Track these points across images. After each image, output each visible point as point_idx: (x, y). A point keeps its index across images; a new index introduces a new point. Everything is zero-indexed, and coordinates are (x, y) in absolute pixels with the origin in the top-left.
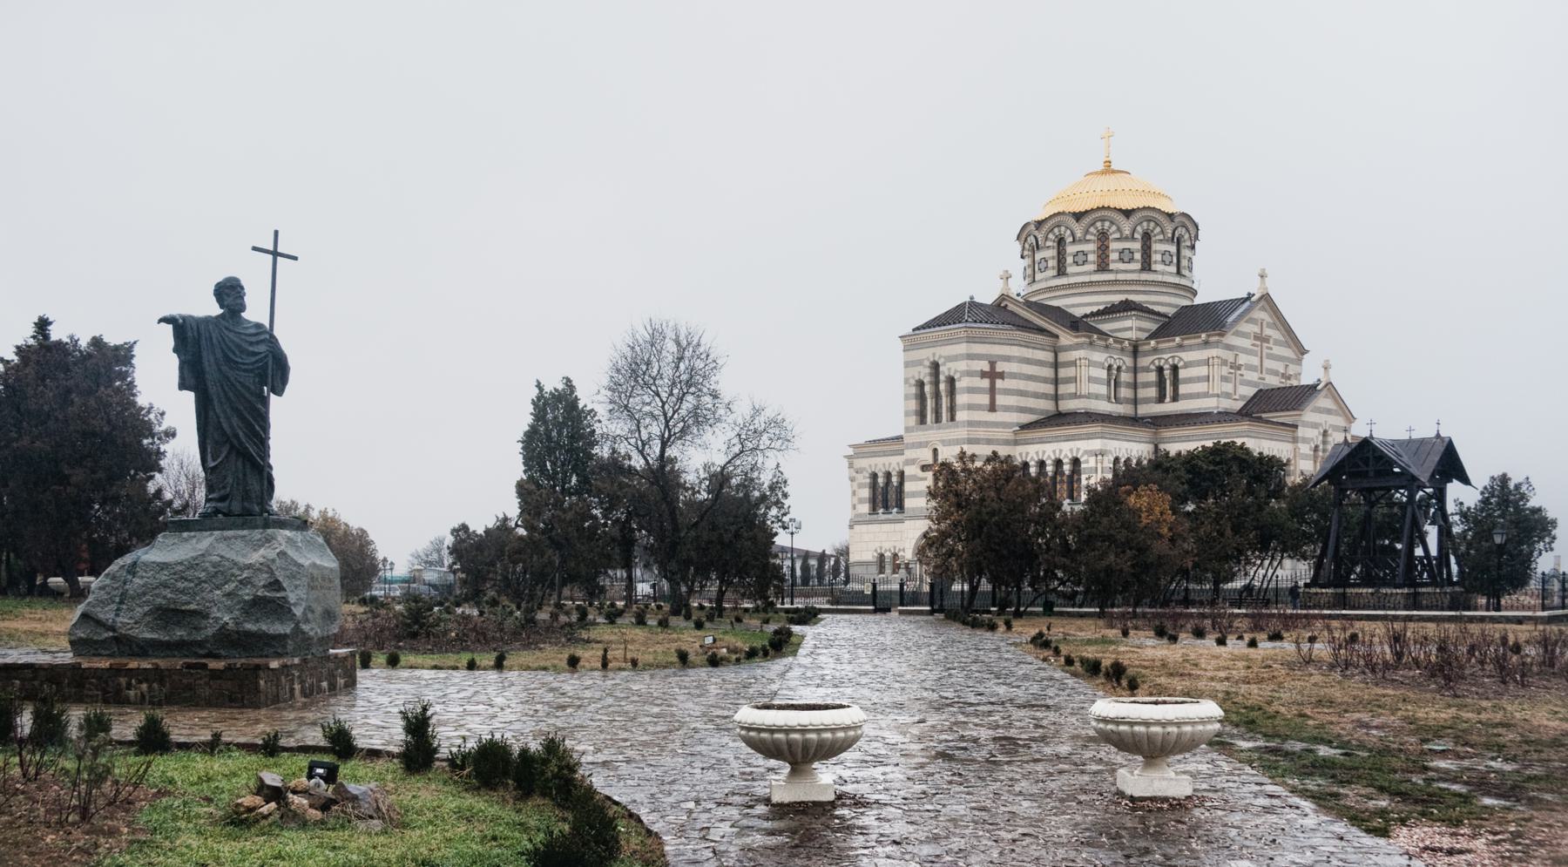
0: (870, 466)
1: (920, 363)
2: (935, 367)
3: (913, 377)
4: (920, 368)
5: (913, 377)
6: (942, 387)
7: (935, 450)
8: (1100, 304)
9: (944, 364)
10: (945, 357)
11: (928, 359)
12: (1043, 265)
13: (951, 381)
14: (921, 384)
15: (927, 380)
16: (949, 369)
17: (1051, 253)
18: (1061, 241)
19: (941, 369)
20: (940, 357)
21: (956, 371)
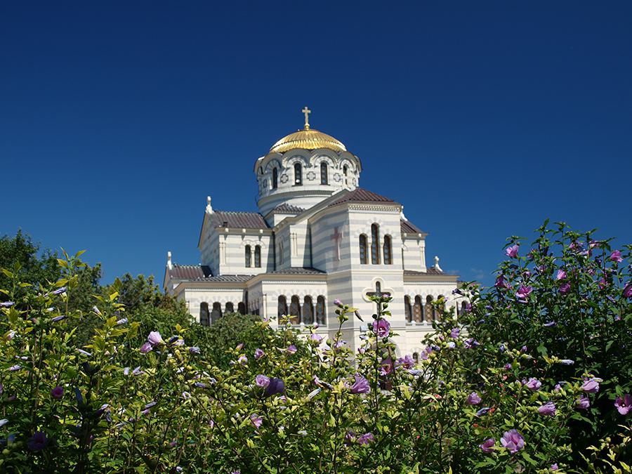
0: (279, 290)
1: (364, 222)
2: (375, 228)
3: (358, 231)
4: (364, 226)
5: (358, 231)
6: (382, 241)
7: (378, 284)
8: (309, 204)
9: (382, 226)
10: (384, 222)
11: (370, 220)
12: (311, 176)
13: (388, 238)
14: (363, 238)
15: (369, 234)
16: (388, 230)
17: (318, 170)
18: (324, 165)
19: (380, 229)
20: (380, 221)
21: (393, 232)
